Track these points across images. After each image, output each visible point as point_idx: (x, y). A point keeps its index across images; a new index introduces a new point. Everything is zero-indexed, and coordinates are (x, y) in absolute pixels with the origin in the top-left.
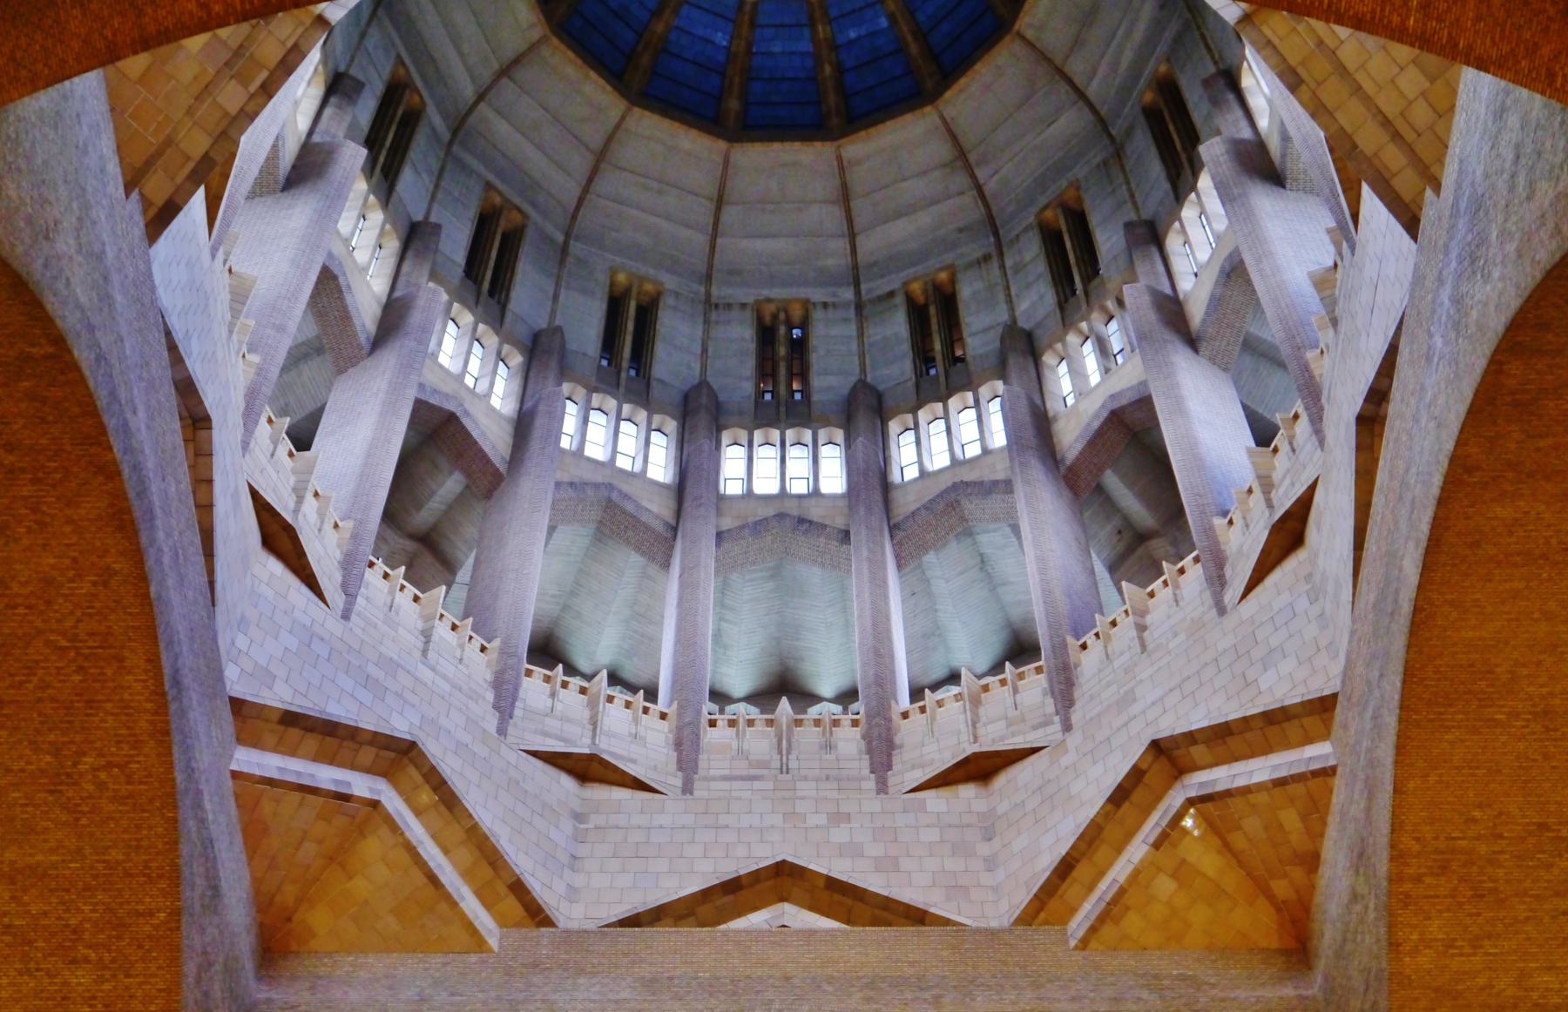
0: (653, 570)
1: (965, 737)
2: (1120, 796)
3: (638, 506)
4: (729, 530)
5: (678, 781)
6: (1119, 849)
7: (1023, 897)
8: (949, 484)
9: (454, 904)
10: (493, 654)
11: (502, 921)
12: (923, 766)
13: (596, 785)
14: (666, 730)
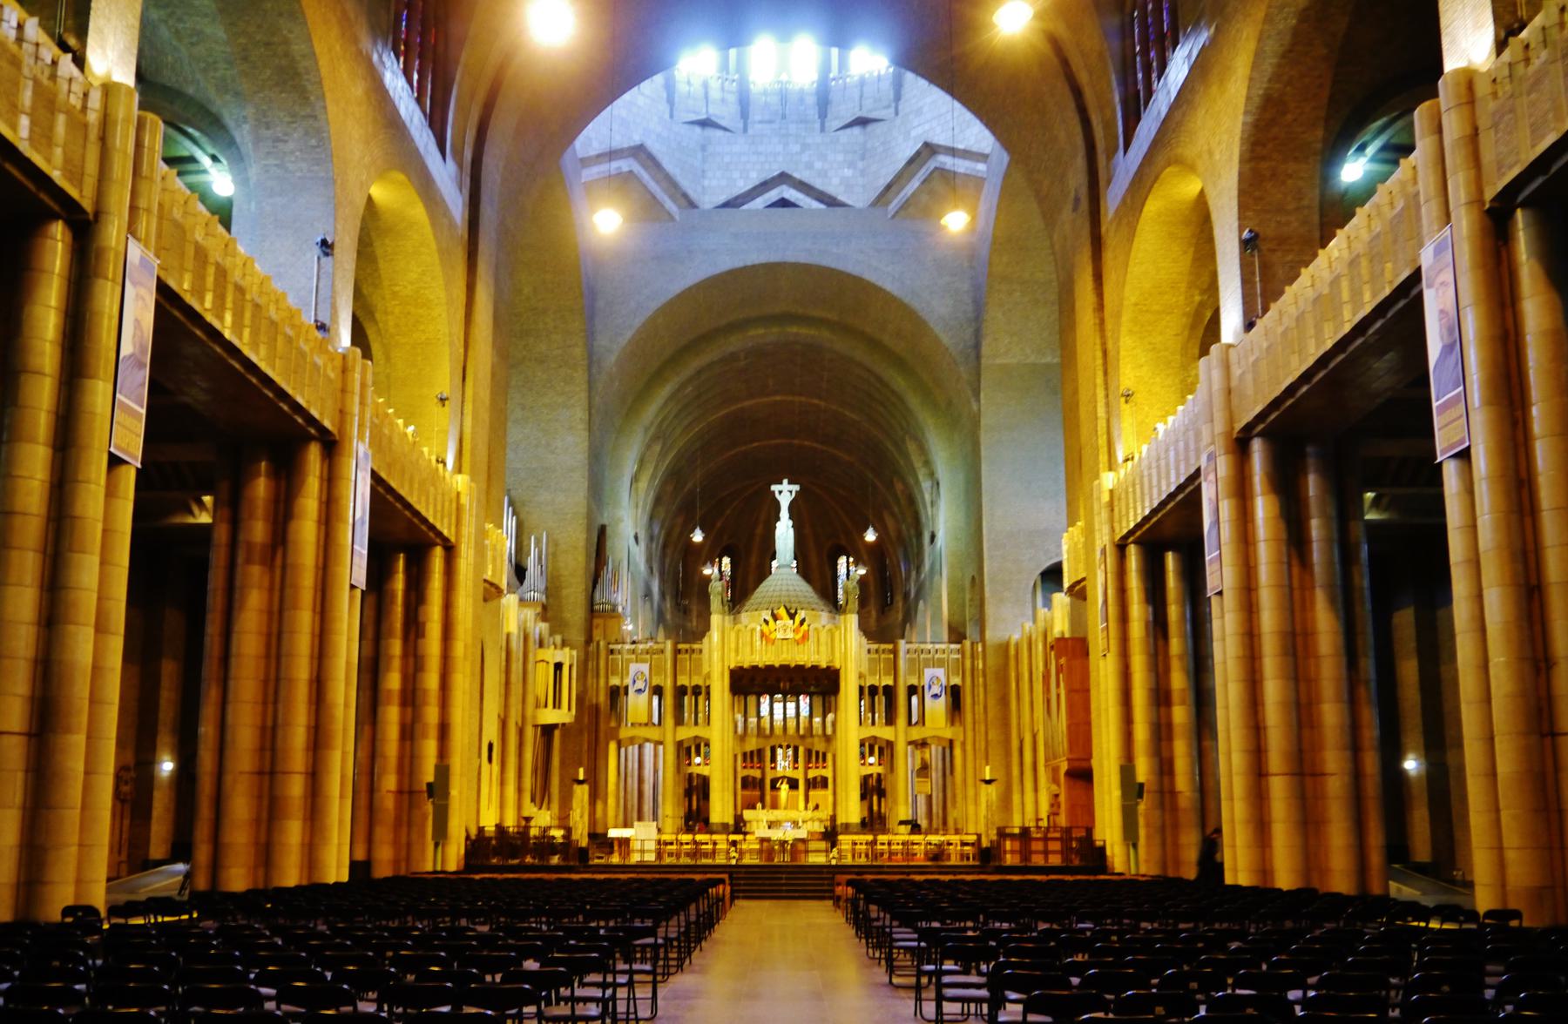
1: (857, 109)
2: (911, 161)
5: (741, 125)
6: (909, 181)
7: (873, 195)
9: (662, 206)
11: (679, 207)
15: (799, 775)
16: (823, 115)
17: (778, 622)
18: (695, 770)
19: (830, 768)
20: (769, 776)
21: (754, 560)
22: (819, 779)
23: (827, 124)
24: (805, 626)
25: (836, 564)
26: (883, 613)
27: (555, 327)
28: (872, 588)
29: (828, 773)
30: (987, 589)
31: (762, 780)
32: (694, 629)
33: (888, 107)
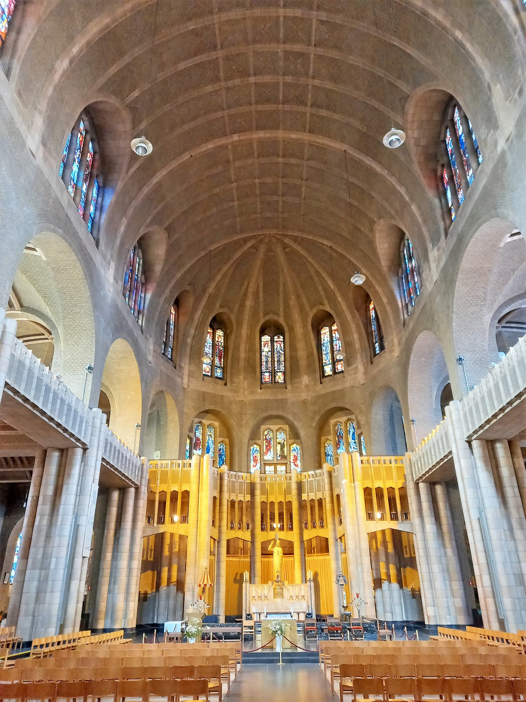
15: (293, 536)
18: (166, 528)
19: (330, 526)
20: (261, 537)
21: (244, 331)
22: (314, 543)
25: (321, 334)
26: (372, 363)
28: (357, 346)
29: (328, 533)
31: (253, 542)
32: (186, 386)
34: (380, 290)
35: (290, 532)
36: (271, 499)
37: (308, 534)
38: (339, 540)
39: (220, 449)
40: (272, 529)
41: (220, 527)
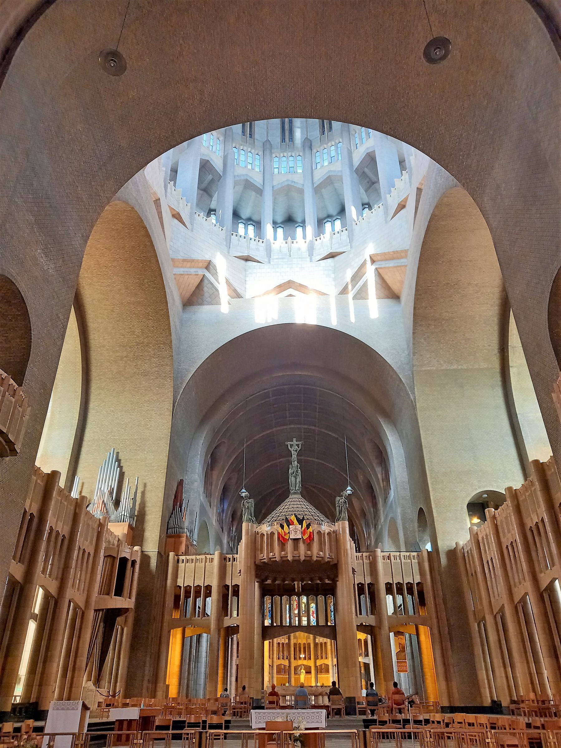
0: (258, 196)
3: (254, 180)
4: (275, 185)
8: (327, 171)
10: (224, 231)
12: (320, 255)
13: (249, 261)
14: (263, 246)
15: (311, 663)
16: (311, 254)
17: (290, 526)
19: (330, 659)
20: (294, 663)
22: (323, 667)
23: (313, 259)
24: (311, 530)
27: (154, 354)
30: (434, 511)
31: (290, 666)
33: (347, 245)
34: (357, 522)
35: (309, 661)
36: (299, 641)
37: (319, 662)
38: (334, 666)
39: (269, 608)
40: (300, 658)
41: (273, 658)
